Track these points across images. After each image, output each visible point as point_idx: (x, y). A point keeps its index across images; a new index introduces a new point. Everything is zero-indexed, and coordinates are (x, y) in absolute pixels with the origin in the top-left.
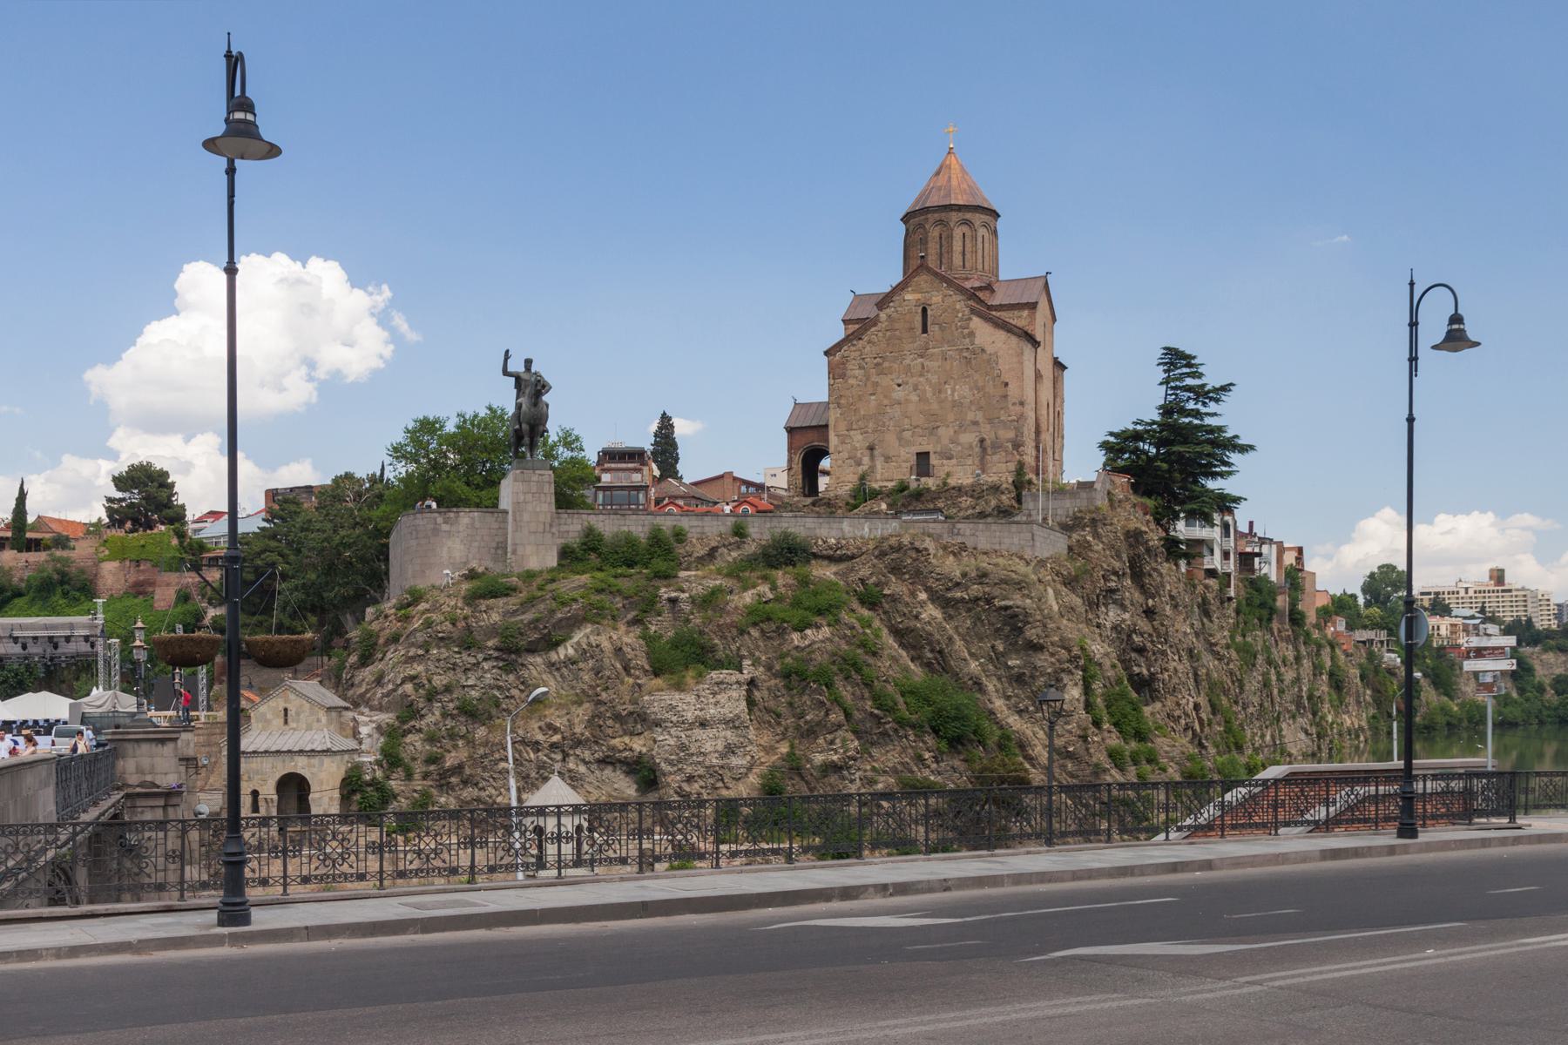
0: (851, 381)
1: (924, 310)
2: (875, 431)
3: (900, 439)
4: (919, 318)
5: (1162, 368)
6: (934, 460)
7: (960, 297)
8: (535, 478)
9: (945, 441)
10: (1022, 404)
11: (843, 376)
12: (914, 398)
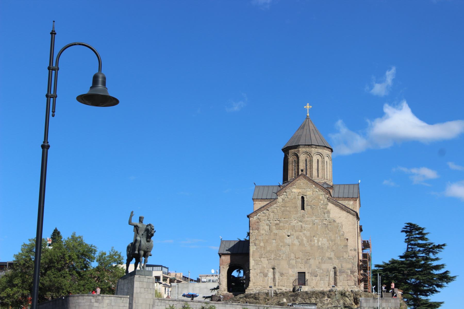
3: (289, 264)
4: (300, 202)
5: (404, 234)
6: (307, 277)
7: (323, 193)
8: (146, 280)
11: (258, 229)
12: (296, 242)
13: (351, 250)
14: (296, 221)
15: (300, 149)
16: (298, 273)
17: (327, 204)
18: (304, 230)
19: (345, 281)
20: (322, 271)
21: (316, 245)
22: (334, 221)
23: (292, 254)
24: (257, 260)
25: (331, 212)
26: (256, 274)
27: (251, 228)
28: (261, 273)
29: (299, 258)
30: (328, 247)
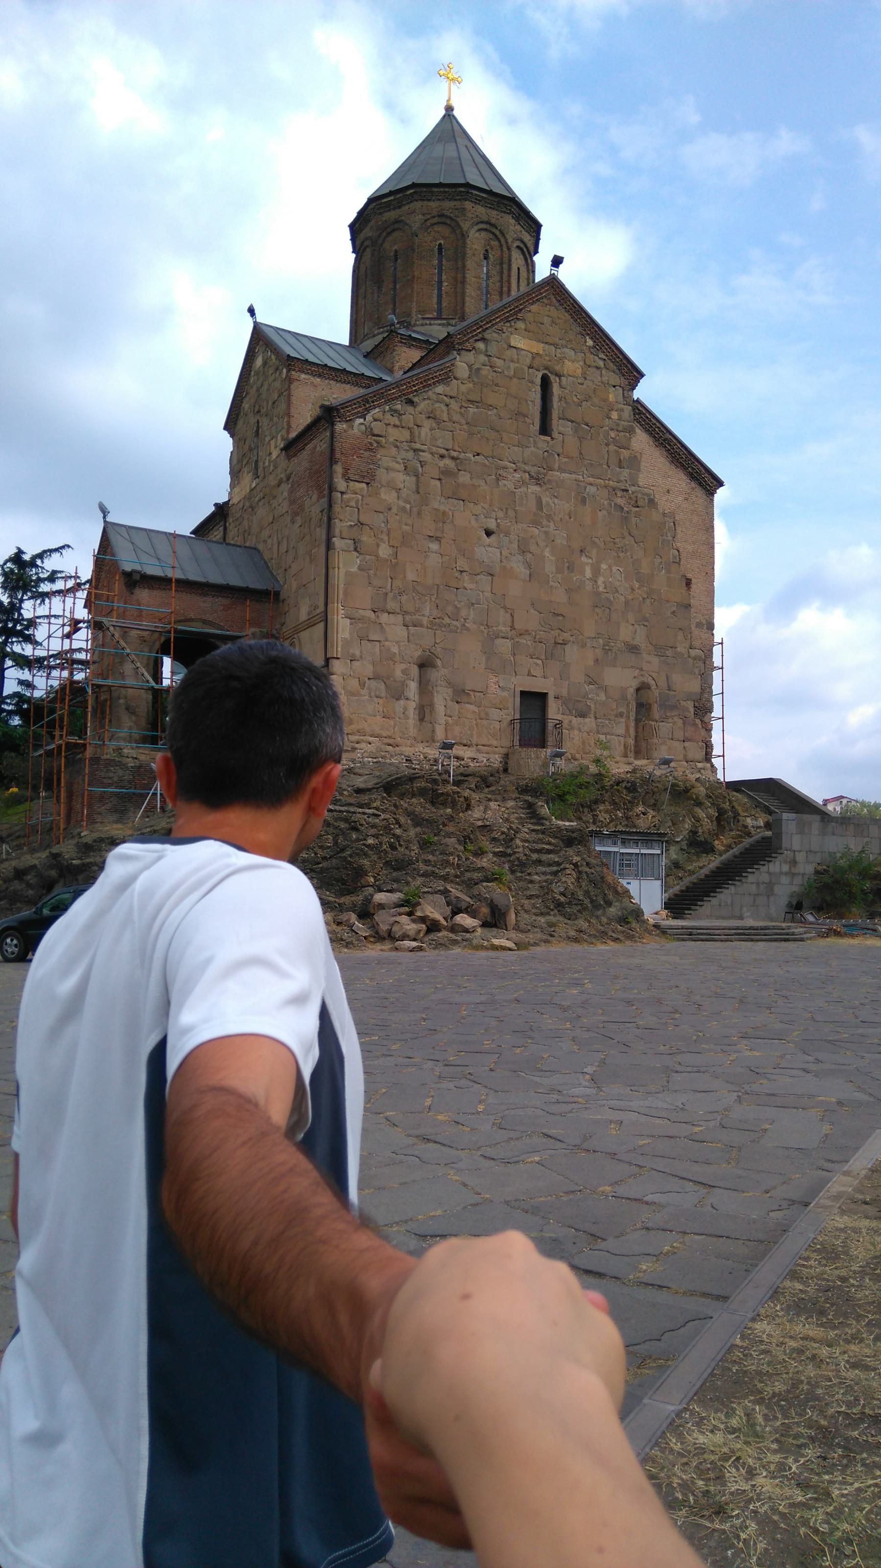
0: (388, 496)
1: (545, 383)
2: (434, 625)
6: (554, 711)
7: (615, 379)
9: (577, 675)
10: (711, 627)
11: (368, 478)
13: (699, 625)
14: (517, 475)
15: (468, 205)
16: (523, 693)
17: (631, 431)
18: (549, 518)
19: (676, 744)
20: (602, 697)
21: (589, 587)
22: (652, 502)
23: (502, 611)
24: (361, 619)
25: (643, 464)
26: (354, 684)
27: (338, 469)
28: (376, 677)
29: (526, 632)
30: (627, 603)
